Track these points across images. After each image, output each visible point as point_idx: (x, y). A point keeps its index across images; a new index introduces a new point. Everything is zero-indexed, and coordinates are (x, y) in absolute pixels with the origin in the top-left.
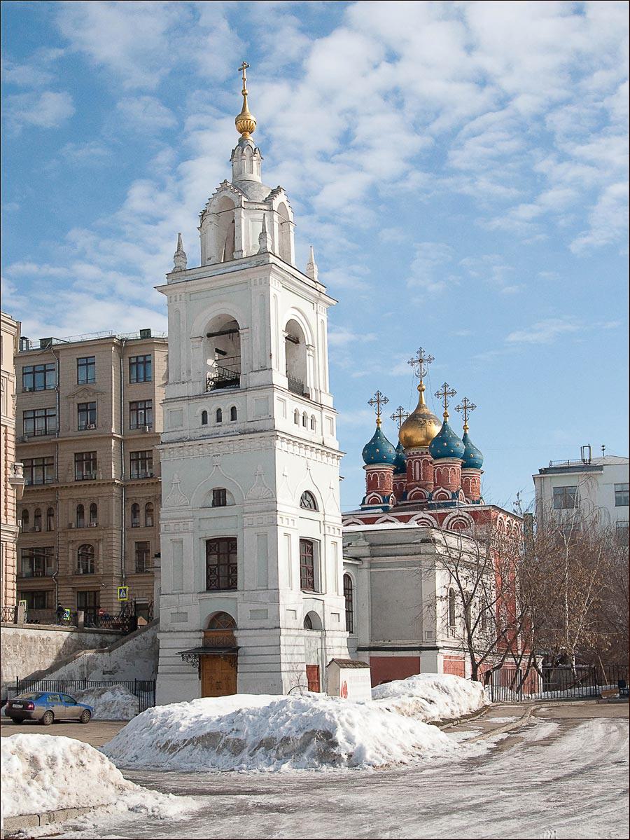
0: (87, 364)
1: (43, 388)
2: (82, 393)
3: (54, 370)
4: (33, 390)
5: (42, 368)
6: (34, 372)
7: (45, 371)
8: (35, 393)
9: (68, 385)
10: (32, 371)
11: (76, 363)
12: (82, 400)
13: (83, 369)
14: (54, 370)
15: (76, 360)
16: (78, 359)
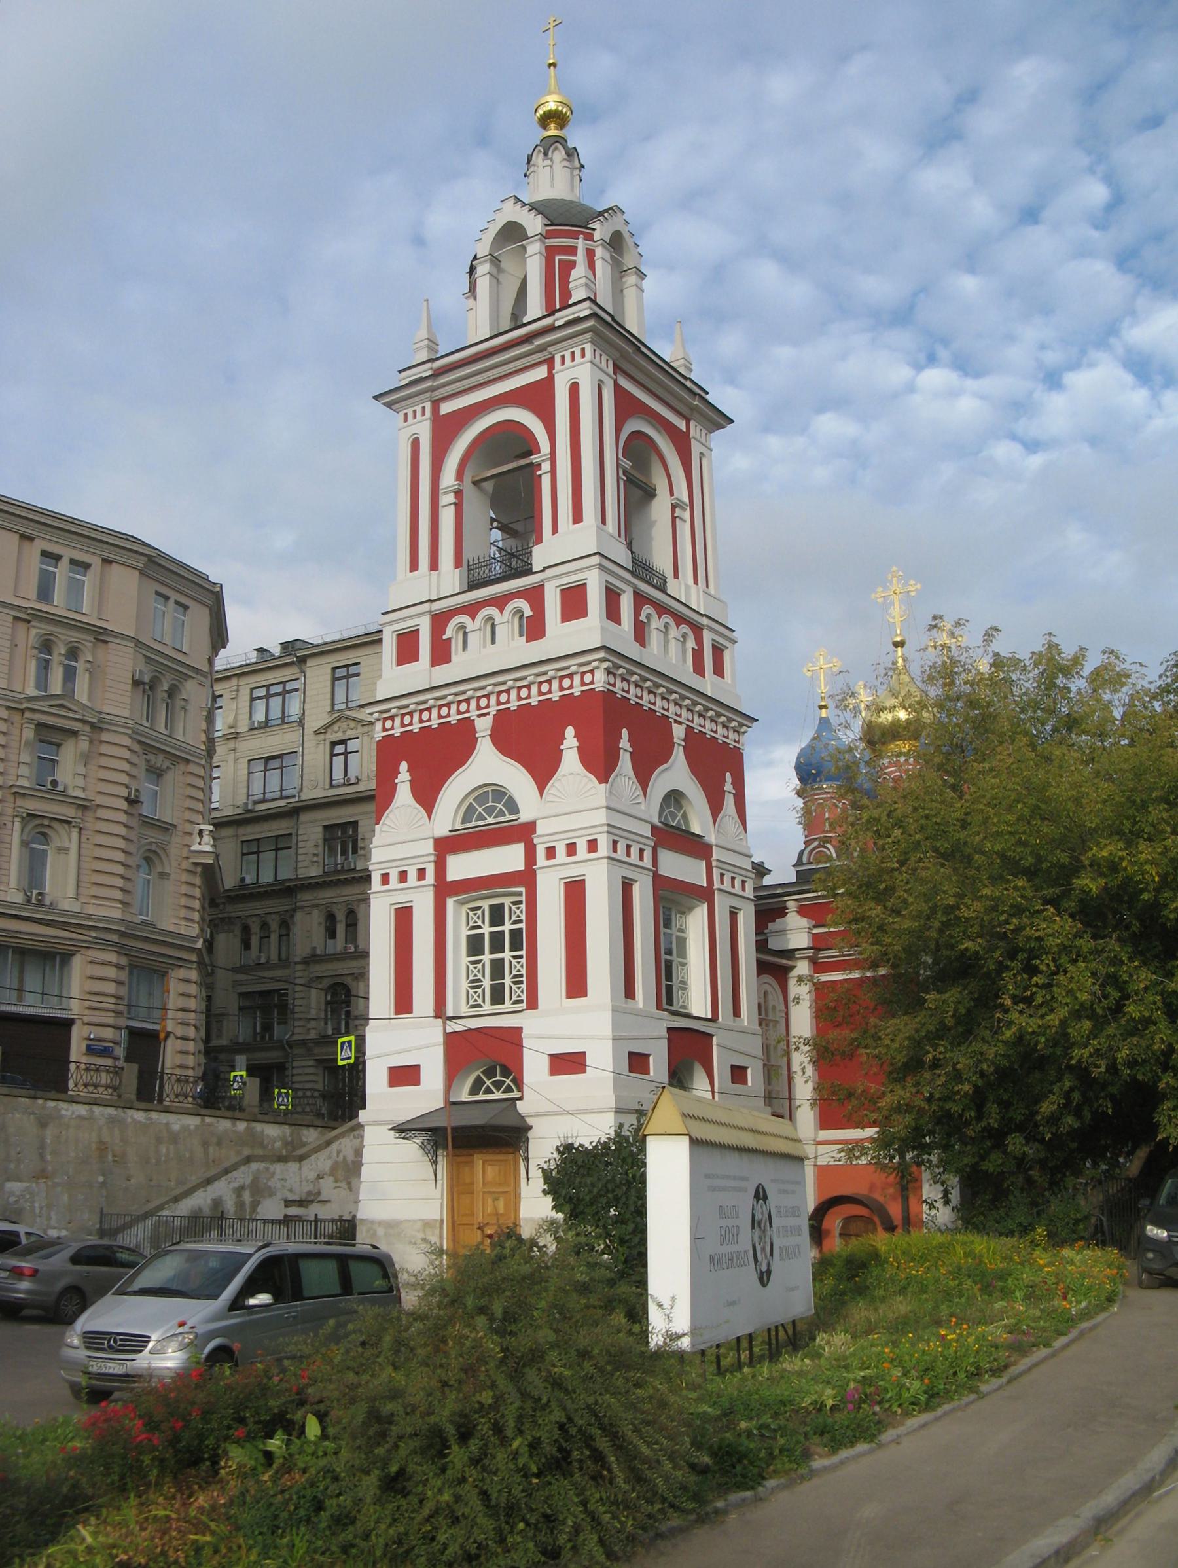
0: (348, 677)
1: (280, 721)
2: (338, 724)
3: (297, 690)
4: (266, 725)
5: (279, 688)
6: (268, 697)
7: (284, 693)
8: (269, 729)
9: (317, 717)
10: (264, 694)
11: (329, 677)
12: (339, 736)
13: (341, 686)
14: (297, 690)
15: (329, 671)
16: (334, 669)
